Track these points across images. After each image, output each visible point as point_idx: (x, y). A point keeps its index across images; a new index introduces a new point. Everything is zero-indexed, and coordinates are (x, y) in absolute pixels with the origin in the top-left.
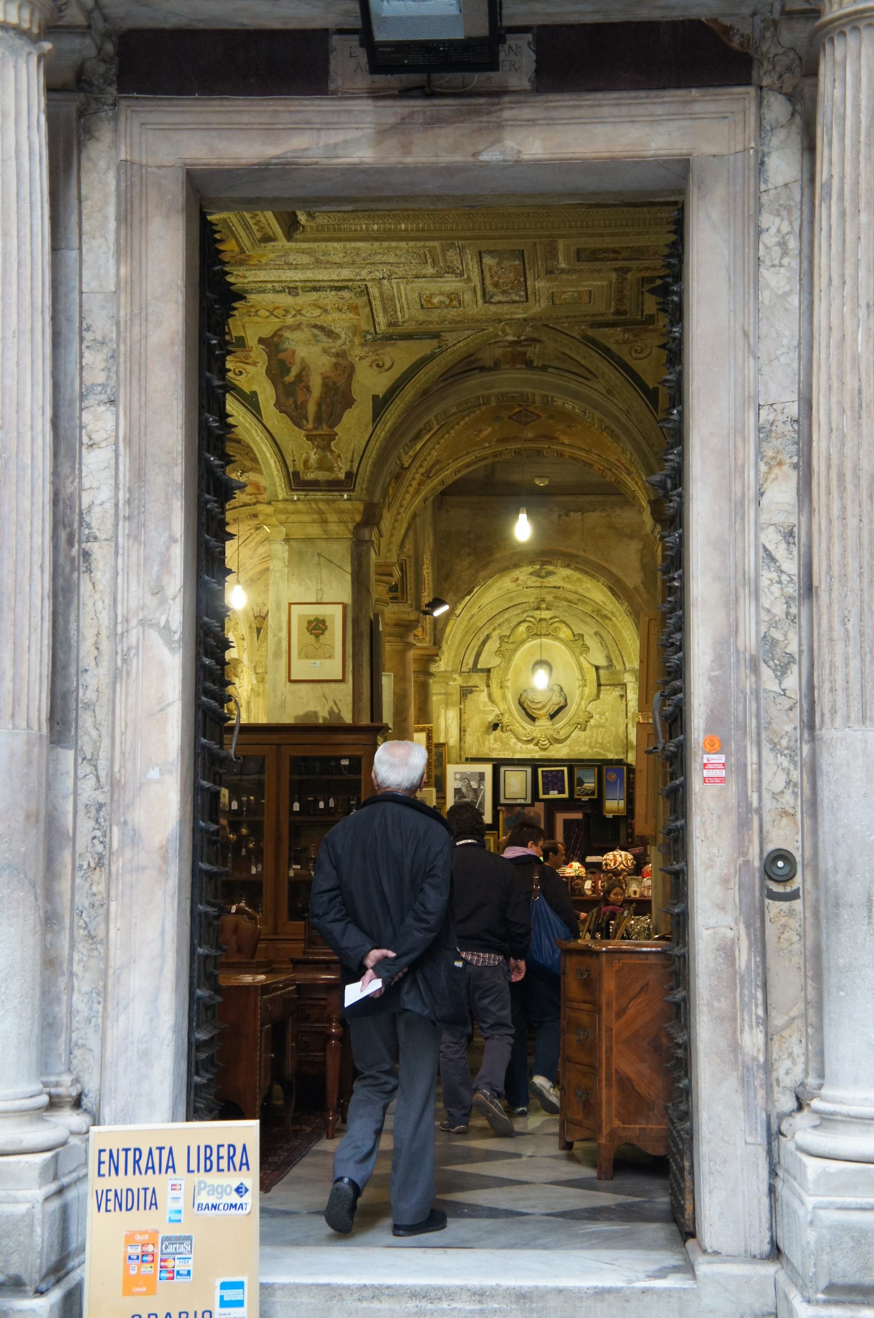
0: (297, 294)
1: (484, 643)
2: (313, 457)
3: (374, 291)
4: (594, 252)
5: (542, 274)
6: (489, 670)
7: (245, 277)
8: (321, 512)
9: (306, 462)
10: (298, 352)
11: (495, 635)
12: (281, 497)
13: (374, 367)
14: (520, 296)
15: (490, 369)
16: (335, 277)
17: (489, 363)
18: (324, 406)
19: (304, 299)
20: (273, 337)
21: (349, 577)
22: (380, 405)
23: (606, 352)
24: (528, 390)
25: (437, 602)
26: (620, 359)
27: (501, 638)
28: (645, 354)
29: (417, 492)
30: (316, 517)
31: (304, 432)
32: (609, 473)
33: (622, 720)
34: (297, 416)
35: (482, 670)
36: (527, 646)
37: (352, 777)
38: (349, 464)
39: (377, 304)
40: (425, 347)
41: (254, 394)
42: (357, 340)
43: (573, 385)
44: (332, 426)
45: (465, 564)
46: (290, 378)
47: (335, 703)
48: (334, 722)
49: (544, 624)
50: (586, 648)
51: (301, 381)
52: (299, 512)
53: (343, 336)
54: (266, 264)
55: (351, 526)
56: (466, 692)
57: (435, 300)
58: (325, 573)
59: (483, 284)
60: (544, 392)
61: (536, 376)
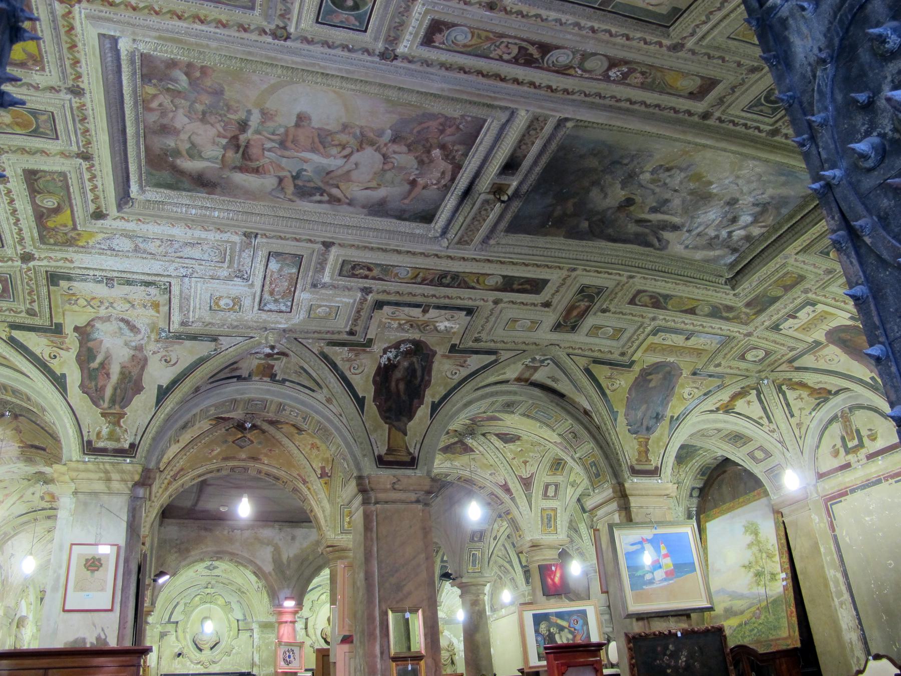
0: (113, 286)
1: (175, 607)
2: (105, 431)
3: (175, 290)
5: (308, 286)
7: (72, 262)
8: (106, 472)
9: (98, 434)
11: (182, 602)
12: (74, 459)
15: (245, 379)
17: (245, 374)
18: (119, 391)
19: (120, 291)
20: (86, 326)
21: (124, 525)
22: (163, 393)
23: (334, 366)
26: (342, 373)
27: (185, 604)
28: (360, 371)
29: (166, 489)
30: (102, 475)
31: (100, 411)
33: (250, 649)
34: (94, 394)
35: (173, 623)
36: (199, 608)
38: (133, 437)
39: (175, 302)
40: (203, 348)
41: (64, 375)
42: (153, 336)
43: (302, 397)
45: (173, 557)
46: (95, 365)
47: (103, 630)
49: (209, 596)
50: (232, 610)
51: (104, 368)
52: (87, 471)
53: (143, 331)
55: (130, 484)
56: (163, 635)
57: (222, 303)
59: (262, 290)
60: (281, 400)
61: (275, 388)
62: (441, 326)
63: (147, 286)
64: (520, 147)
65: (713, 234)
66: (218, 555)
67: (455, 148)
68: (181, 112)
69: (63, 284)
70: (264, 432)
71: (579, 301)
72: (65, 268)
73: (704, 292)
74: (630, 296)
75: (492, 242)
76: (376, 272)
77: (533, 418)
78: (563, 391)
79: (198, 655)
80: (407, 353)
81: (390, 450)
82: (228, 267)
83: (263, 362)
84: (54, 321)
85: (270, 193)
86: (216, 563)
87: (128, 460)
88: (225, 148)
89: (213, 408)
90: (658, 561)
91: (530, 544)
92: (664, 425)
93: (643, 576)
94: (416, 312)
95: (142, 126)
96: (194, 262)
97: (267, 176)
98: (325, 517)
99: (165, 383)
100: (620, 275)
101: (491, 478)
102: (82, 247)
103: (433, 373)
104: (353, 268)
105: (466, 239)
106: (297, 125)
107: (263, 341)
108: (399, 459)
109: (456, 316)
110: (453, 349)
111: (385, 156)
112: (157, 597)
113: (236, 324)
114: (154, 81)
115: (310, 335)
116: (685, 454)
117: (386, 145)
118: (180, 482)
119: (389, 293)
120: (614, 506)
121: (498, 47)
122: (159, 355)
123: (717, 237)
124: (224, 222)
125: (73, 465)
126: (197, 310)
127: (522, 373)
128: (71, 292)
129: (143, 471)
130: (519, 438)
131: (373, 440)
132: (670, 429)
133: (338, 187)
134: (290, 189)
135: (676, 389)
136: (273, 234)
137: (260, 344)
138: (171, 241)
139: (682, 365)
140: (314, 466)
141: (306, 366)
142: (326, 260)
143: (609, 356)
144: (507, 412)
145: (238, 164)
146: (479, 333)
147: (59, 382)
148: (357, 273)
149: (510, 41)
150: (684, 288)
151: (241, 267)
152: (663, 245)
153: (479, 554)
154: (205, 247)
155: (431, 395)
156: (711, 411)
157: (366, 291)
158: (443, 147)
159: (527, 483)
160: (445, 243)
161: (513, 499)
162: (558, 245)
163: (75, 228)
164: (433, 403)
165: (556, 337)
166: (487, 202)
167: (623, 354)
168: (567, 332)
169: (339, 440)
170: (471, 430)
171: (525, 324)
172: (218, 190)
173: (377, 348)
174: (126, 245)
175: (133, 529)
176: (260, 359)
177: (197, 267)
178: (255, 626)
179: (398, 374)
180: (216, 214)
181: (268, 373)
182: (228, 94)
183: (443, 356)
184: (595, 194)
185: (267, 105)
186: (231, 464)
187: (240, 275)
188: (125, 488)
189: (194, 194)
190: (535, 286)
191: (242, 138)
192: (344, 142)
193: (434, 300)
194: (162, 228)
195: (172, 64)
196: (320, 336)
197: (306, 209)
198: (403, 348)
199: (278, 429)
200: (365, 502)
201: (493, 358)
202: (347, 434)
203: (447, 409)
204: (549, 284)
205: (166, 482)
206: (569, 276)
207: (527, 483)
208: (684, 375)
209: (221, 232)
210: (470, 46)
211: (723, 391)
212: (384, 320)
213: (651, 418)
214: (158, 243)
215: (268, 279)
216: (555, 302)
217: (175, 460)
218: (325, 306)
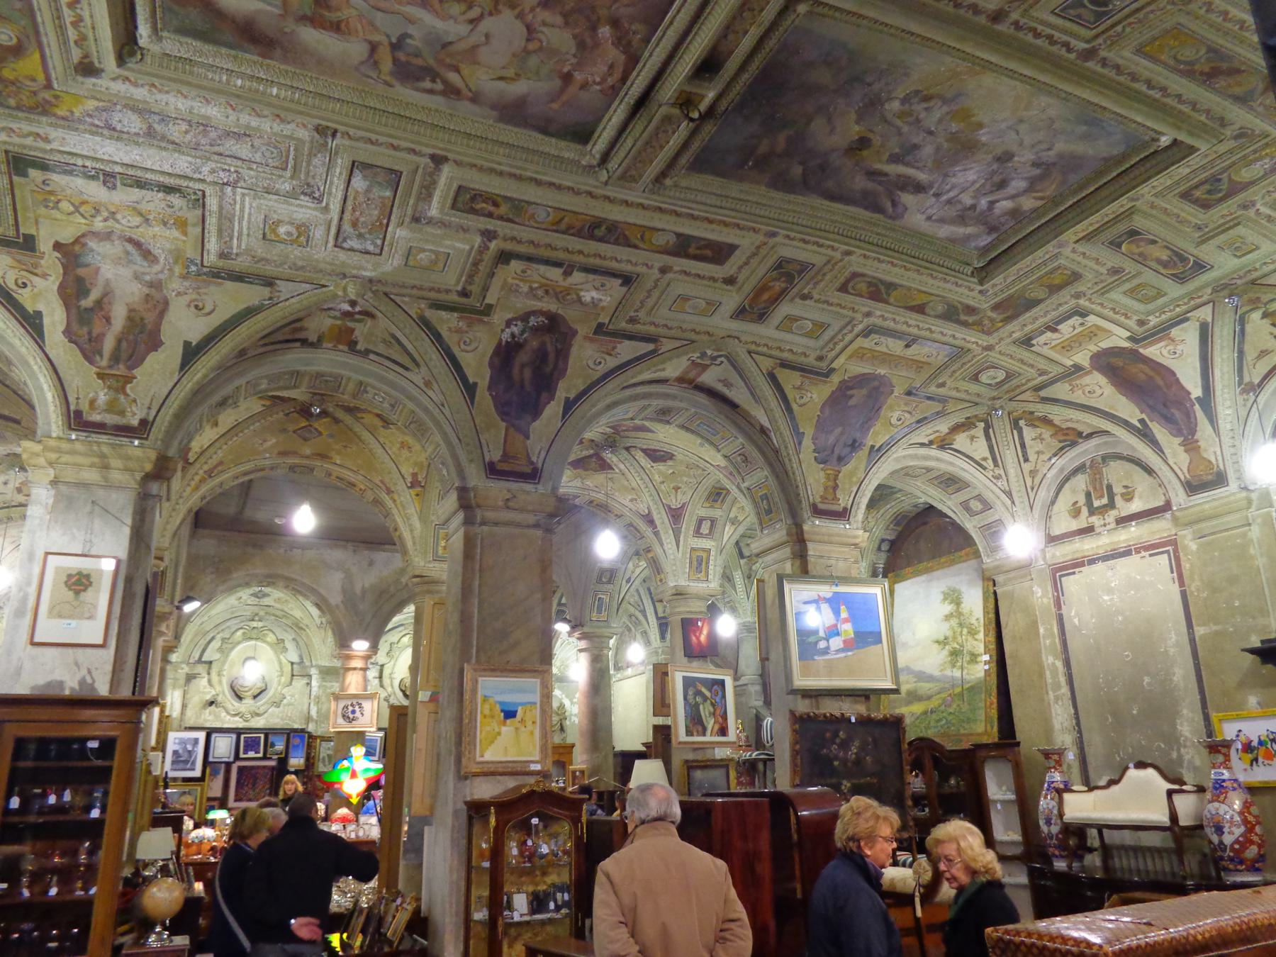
0: (114, 187)
1: (209, 643)
2: (103, 398)
3: (212, 203)
4: (477, 196)
5: (407, 220)
6: (211, 662)
9: (92, 402)
10: (102, 270)
12: (54, 435)
13: (193, 309)
14: (375, 245)
15: (312, 345)
16: (167, 168)
17: (313, 338)
18: (124, 344)
19: (124, 196)
20: (73, 243)
21: (127, 531)
22: (191, 353)
23: (437, 337)
24: (343, 372)
25: (189, 599)
27: (223, 639)
29: (197, 488)
30: (96, 460)
31: (95, 369)
32: (369, 492)
33: (306, 701)
35: (205, 662)
37: (99, 763)
38: (145, 411)
39: (212, 222)
40: (252, 295)
41: (39, 314)
42: (178, 270)
43: (391, 376)
44: (131, 368)
45: (208, 579)
46: (87, 302)
47: (89, 672)
48: (86, 694)
50: (285, 650)
51: (101, 309)
52: (73, 452)
53: (162, 260)
54: (80, 121)
55: (138, 476)
56: (190, 678)
57: (282, 230)
58: (97, 523)
59: (341, 219)
60: (361, 378)
62: (588, 296)
63: (168, 193)
64: (725, 36)
65: (967, 200)
66: (271, 579)
67: (633, 28)
69: (33, 173)
70: (337, 421)
71: (774, 280)
72: (36, 149)
73: (941, 284)
74: (842, 280)
75: (668, 182)
76: (504, 209)
77: (693, 432)
78: (736, 400)
79: (236, 704)
80: (536, 330)
81: (506, 457)
82: (292, 178)
83: (339, 322)
84: (22, 231)
85: (357, 69)
86: (267, 590)
87: (136, 443)
89: (265, 381)
90: (835, 626)
91: (674, 591)
92: (861, 457)
93: (816, 643)
94: (555, 274)
96: (239, 163)
98: (413, 537)
99: (195, 338)
100: (832, 248)
101: (630, 505)
102: (63, 118)
103: (571, 361)
104: (473, 199)
105: (634, 173)
107: (340, 293)
108: (517, 469)
109: (608, 285)
110: (600, 329)
111: (529, 28)
112: (183, 628)
113: (300, 263)
115: (408, 291)
116: (882, 494)
117: (532, 9)
118: (218, 480)
119: (520, 242)
120: (787, 551)
122: (188, 298)
123: (973, 207)
124: (286, 104)
125: (52, 443)
126: (245, 238)
127: (686, 372)
128: (48, 189)
129: (158, 459)
130: (671, 457)
131: (483, 441)
132: (869, 462)
133: (457, 71)
134: (387, 65)
135: (882, 412)
136: (360, 133)
137: (335, 296)
138: (205, 125)
139: (894, 381)
140: (403, 471)
141: (399, 334)
142: (434, 183)
143: (802, 359)
144: (661, 421)
145: (309, 13)
146: (636, 311)
147: (32, 323)
148: (478, 207)
150: (915, 275)
151: (310, 180)
152: (898, 211)
153: (606, 598)
154: (257, 142)
155: (565, 389)
156: (922, 445)
157: (489, 235)
158: (615, 23)
159: (676, 515)
160: (604, 176)
161: (657, 534)
162: (757, 194)
163: (49, 86)
164: (567, 399)
165: (735, 326)
166: (667, 119)
167: (820, 358)
168: (753, 321)
169: (438, 438)
170: (611, 442)
171: (699, 303)
172: (278, 52)
173: (498, 318)
174: (133, 123)
175: (140, 537)
176: (335, 318)
177: (245, 172)
178: (313, 671)
179: (523, 357)
180: (275, 91)
181: (344, 338)
183: (586, 338)
184: (818, 125)
186: (292, 460)
187: (308, 191)
188: (131, 481)
189: (240, 54)
190: (719, 253)
193: (581, 259)
194: (189, 103)
196: (420, 293)
197: (410, 100)
198: (533, 321)
199: (357, 419)
200: (468, 522)
201: (651, 347)
202: (449, 430)
203: (584, 409)
204: (737, 252)
205: (197, 478)
206: (765, 244)
207: (676, 515)
208: (896, 394)
209: (282, 121)
211: (943, 419)
212: (510, 280)
213: (845, 445)
214: (184, 127)
216: (741, 278)
217: (212, 450)
218: (430, 251)
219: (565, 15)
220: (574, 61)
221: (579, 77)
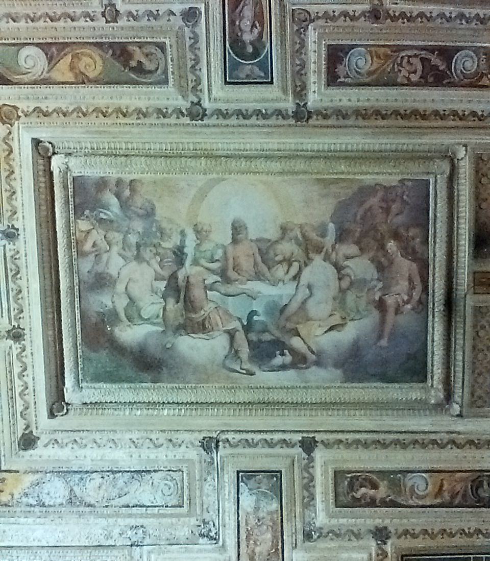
68: (115, 249)
76: (382, 492)
88: (164, 297)
95: (76, 281)
97: (216, 333)
106: (235, 241)
111: (338, 268)
114: (87, 212)
117: (333, 247)
121: (400, 65)
134: (245, 351)
142: (312, 479)
148: (358, 495)
149: (410, 53)
157: (381, 534)
158: (396, 236)
180: (166, 412)
182: (160, 213)
185: (199, 219)
191: (181, 275)
192: (288, 255)
195: (102, 184)
210: (374, 72)
215: (243, 531)
219: (357, 243)
220: (380, 285)
221: (390, 301)
